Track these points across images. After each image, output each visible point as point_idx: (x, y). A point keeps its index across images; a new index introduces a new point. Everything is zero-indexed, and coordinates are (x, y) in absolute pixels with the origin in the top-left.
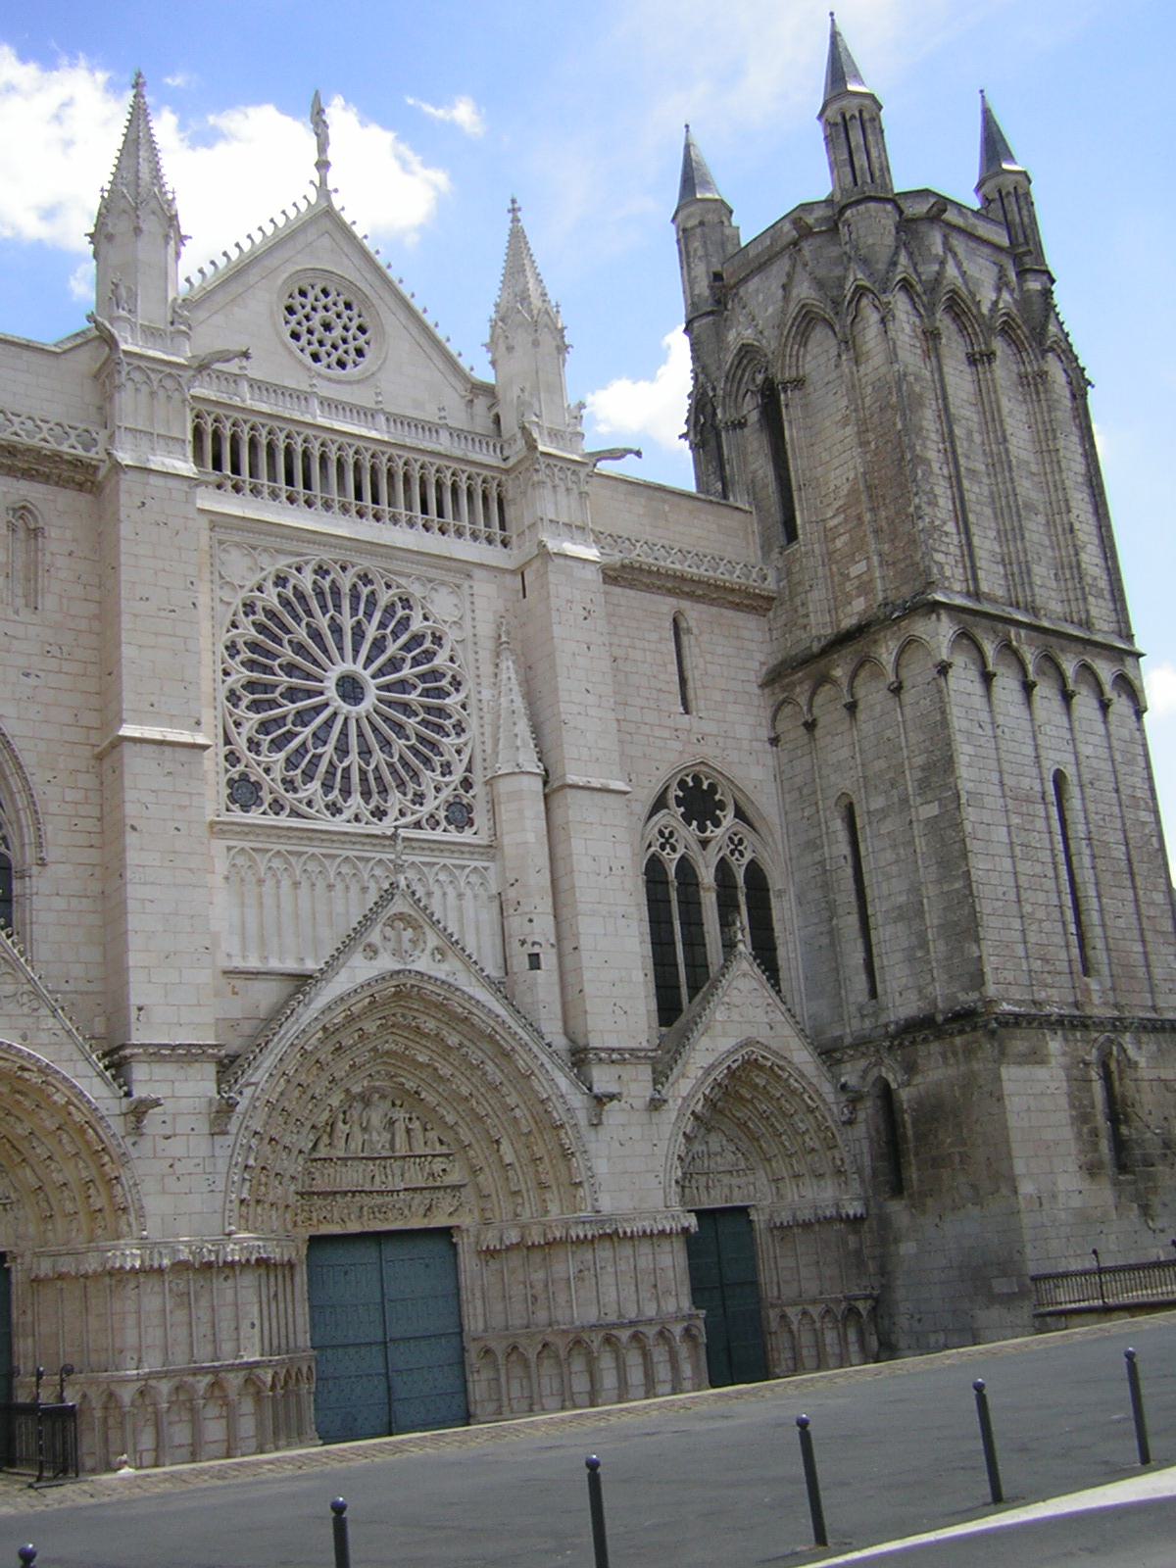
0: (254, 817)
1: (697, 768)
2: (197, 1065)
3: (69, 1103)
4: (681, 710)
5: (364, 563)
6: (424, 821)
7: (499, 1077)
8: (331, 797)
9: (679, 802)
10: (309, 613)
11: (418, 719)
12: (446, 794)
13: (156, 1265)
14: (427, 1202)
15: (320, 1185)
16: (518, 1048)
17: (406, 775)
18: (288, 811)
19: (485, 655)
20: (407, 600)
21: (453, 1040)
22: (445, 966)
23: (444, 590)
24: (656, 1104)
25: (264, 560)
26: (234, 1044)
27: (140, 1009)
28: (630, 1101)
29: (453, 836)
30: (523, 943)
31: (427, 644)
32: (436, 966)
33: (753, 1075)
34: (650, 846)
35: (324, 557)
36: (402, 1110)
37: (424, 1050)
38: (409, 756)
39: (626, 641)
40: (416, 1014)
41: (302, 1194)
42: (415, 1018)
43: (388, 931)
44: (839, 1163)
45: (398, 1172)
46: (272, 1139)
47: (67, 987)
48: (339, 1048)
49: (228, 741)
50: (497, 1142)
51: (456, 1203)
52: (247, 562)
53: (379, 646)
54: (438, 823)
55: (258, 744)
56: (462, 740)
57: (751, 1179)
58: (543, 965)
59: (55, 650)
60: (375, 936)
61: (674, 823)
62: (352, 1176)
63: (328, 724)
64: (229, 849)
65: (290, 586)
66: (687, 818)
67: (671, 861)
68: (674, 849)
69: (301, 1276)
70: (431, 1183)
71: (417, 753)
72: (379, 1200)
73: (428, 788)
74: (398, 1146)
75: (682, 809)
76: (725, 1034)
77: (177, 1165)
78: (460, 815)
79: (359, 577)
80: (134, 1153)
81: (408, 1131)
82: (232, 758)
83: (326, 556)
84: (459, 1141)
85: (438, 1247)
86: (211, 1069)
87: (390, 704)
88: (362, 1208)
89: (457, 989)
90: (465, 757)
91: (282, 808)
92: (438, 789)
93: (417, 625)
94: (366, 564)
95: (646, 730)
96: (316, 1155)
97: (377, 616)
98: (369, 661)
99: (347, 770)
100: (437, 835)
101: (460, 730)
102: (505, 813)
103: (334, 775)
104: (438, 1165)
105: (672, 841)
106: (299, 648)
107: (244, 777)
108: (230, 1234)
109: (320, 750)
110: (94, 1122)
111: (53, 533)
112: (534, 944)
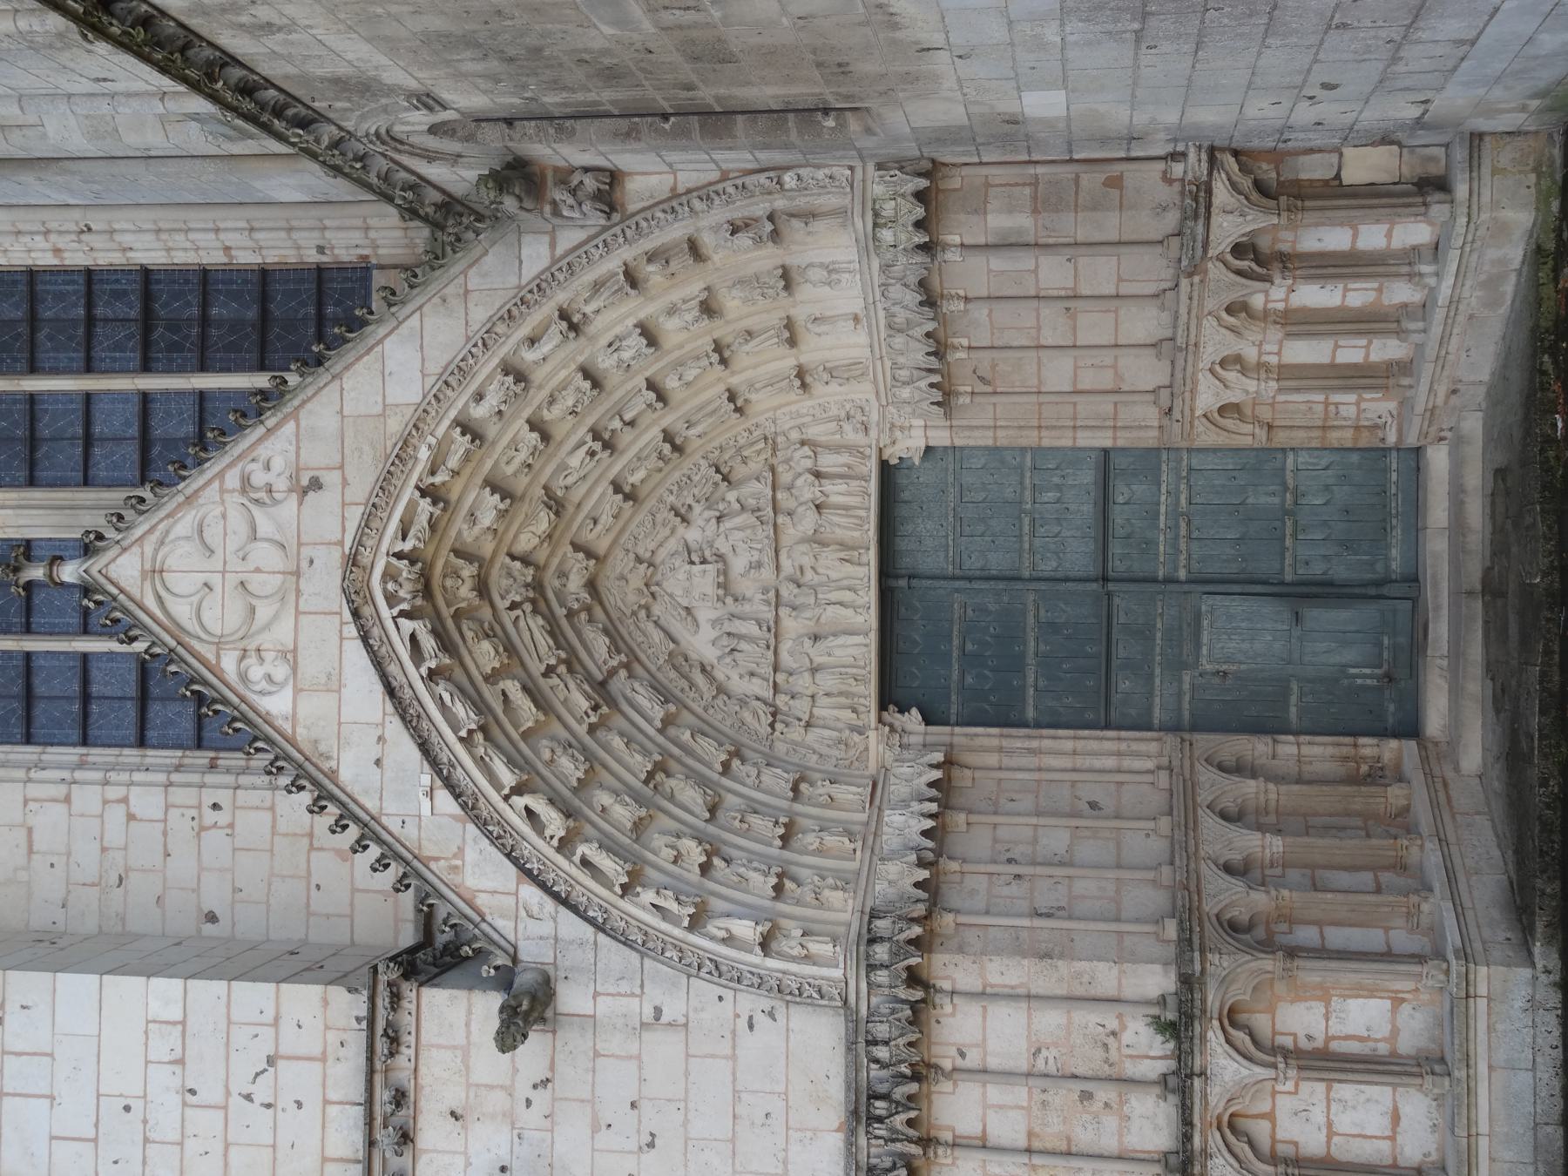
33: (469, 536)
44: (744, 240)
76: (334, 684)
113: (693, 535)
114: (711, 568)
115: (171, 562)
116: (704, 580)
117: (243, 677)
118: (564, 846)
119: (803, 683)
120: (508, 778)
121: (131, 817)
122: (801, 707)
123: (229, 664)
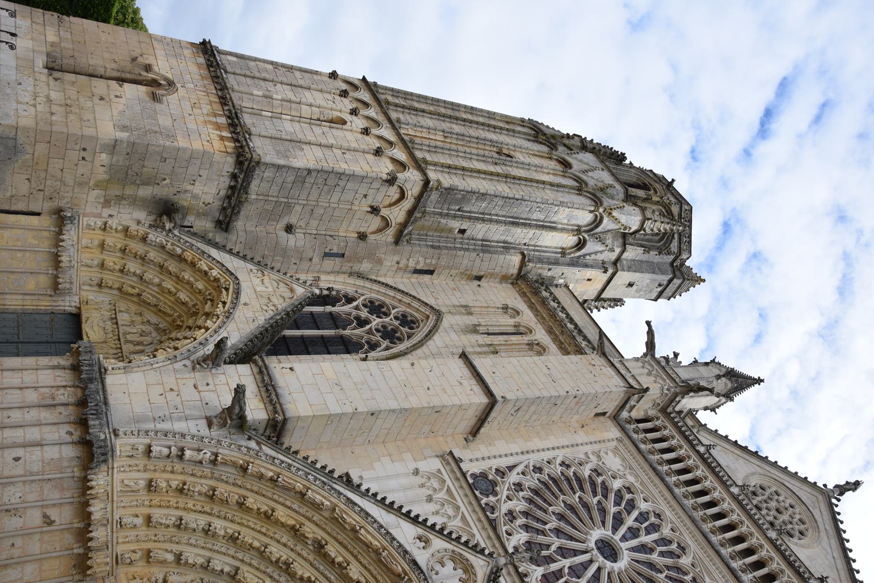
2: (262, 406)
35: (668, 513)
43: (450, 565)
49: (511, 468)
60: (438, 544)
64: (439, 471)
77: (174, 394)
82: (500, 472)
83: (668, 513)
94: (690, 543)
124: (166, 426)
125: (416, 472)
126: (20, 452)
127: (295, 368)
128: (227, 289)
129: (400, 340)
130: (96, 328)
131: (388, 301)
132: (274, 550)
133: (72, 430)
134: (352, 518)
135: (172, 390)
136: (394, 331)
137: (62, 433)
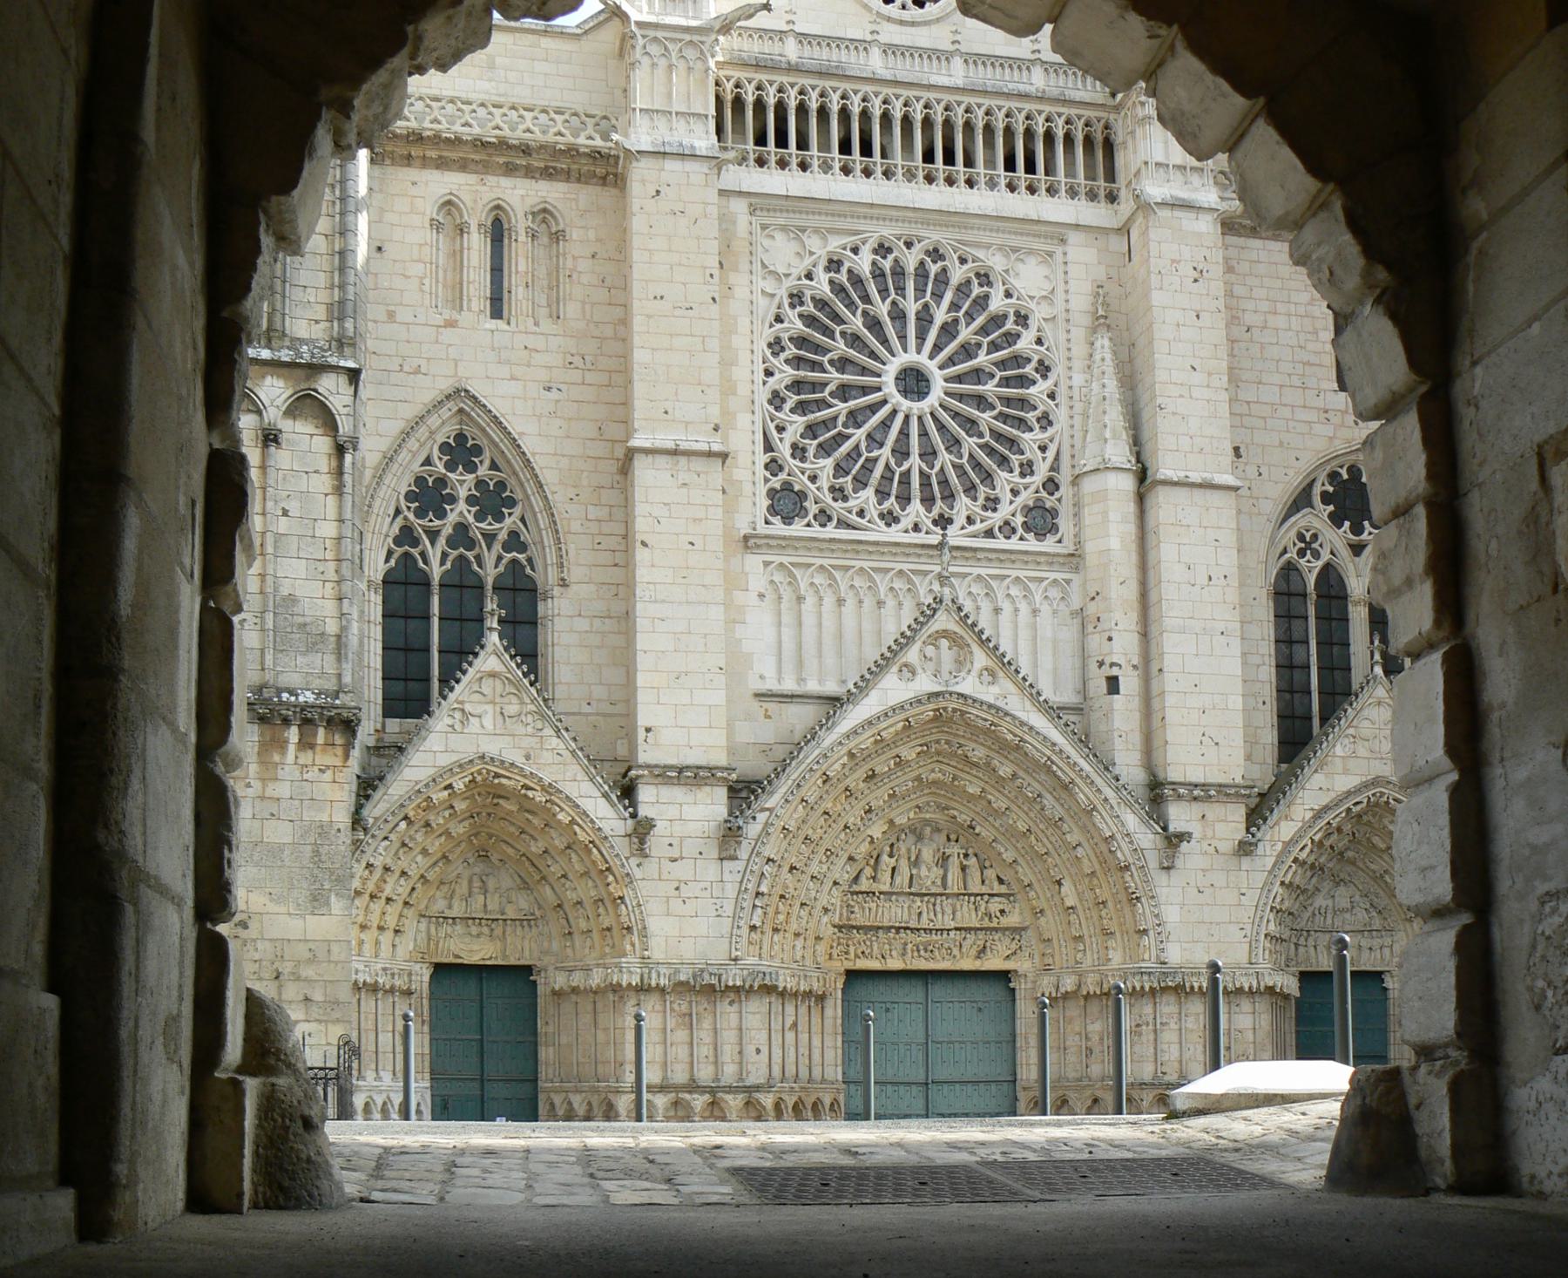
0: (797, 529)
1: (1353, 457)
2: (708, 789)
3: (573, 822)
4: (1335, 386)
5: (933, 236)
6: (996, 530)
7: (1059, 812)
8: (886, 505)
9: (1326, 498)
10: (866, 299)
11: (995, 412)
12: (1026, 497)
13: (653, 983)
14: (981, 943)
15: (859, 919)
16: (1078, 780)
17: (977, 477)
18: (835, 521)
19: (1078, 334)
20: (986, 276)
21: (1005, 770)
22: (995, 689)
23: (1032, 261)
24: (1245, 849)
25: (813, 243)
26: (753, 765)
27: (648, 730)
28: (1215, 843)
29: (1032, 544)
30: (1101, 664)
31: (1009, 325)
32: (984, 688)
33: (1386, 821)
34: (1285, 551)
36: (958, 845)
37: (975, 780)
38: (982, 456)
39: (1265, 306)
40: (962, 741)
41: (840, 928)
42: (961, 746)
43: (930, 650)
45: (949, 910)
46: (792, 868)
47: (587, 709)
48: (871, 776)
49: (769, 448)
50: (1059, 883)
51: (1014, 946)
52: (794, 246)
53: (949, 330)
54: (1014, 531)
55: (804, 450)
56: (1047, 435)
57: (1388, 941)
58: (1122, 691)
59: (577, 361)
60: (912, 655)
61: (1317, 524)
62: (894, 912)
63: (885, 425)
64: (767, 564)
65: (844, 270)
66: (1336, 519)
67: (1311, 570)
68: (1316, 555)
69: (834, 1009)
70: (986, 923)
71: (991, 452)
72: (924, 937)
73: (1002, 489)
74: (950, 883)
75: (1331, 508)
76: (1346, 772)
78: (1041, 520)
79: (928, 253)
80: (638, 873)
81: (963, 868)
82: (774, 466)
83: (887, 232)
84: (1020, 881)
85: (993, 992)
86: (722, 793)
87: (961, 397)
88: (906, 944)
89: (1007, 714)
90: (1050, 454)
91: (830, 519)
92: (1015, 493)
93: (997, 303)
95: (1286, 412)
96: (855, 888)
97: (948, 297)
98: (937, 348)
99: (906, 475)
100: (1014, 544)
101: (1046, 421)
102: (1090, 516)
103: (892, 480)
104: (995, 905)
105: (1314, 546)
106: (854, 340)
107: (787, 486)
108: (736, 959)
109: (875, 454)
110: (597, 842)
111: (575, 234)
112: (1112, 665)
113: (1357, 898)
114: (1349, 906)
115: (1382, 708)
116: (1345, 903)
117: (1346, 736)
118: (1296, 860)
119: (1311, 942)
120: (1317, 838)
121: (1258, 666)
122: (1302, 941)
123: (1351, 731)
124: (729, 909)
125: (761, 596)
126: (750, 1050)
127: (649, 725)
128: (497, 776)
129: (501, 485)
130: (476, 947)
131: (416, 467)
132: (852, 820)
133: (728, 1000)
134: (866, 740)
135: (677, 889)
136: (480, 484)
137: (728, 1012)
